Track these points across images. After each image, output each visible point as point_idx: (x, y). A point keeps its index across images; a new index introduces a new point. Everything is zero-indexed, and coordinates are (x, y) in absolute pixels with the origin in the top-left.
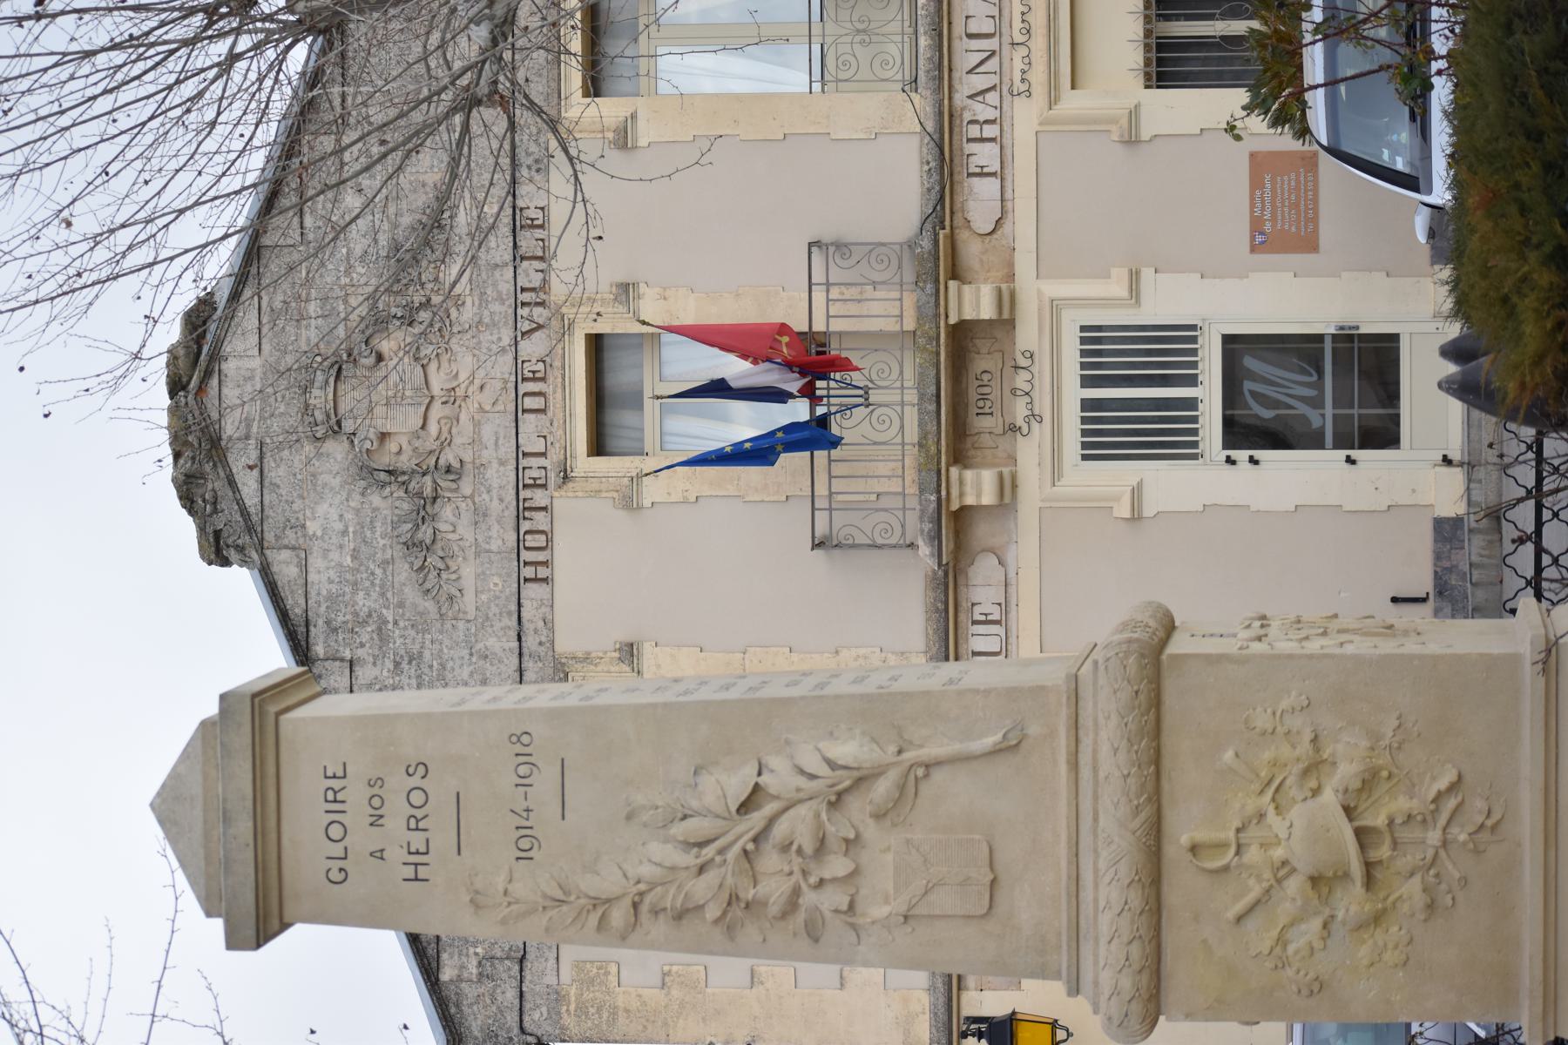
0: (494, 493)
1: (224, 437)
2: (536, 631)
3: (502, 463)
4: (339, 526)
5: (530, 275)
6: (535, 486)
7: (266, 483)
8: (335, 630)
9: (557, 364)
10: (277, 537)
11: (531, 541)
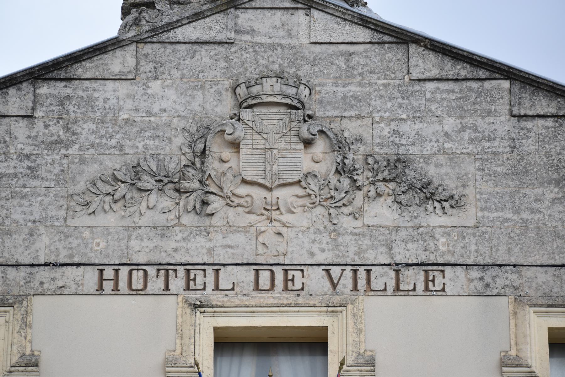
0: (183, 244)
1: (238, 12)
2: (54, 279)
3: (210, 251)
4: (156, 108)
5: (383, 278)
6: (188, 280)
7: (196, 47)
8: (61, 104)
9: (300, 300)
10: (147, 55)
11: (138, 276)
